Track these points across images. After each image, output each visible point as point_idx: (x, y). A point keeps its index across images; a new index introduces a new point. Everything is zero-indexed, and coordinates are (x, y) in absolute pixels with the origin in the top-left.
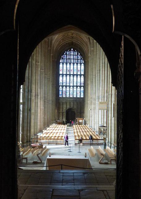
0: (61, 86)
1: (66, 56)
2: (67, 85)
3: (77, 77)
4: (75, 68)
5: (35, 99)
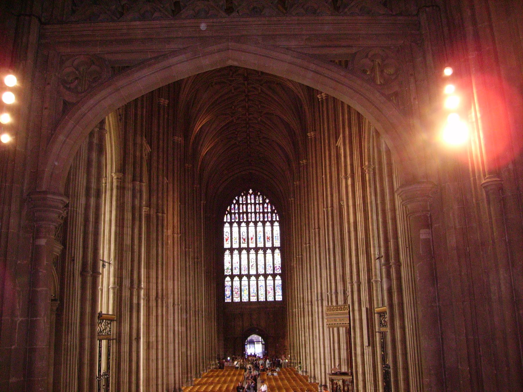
0: (229, 276)
1: (236, 206)
2: (243, 273)
3: (265, 254)
4: (260, 234)
5: (157, 306)
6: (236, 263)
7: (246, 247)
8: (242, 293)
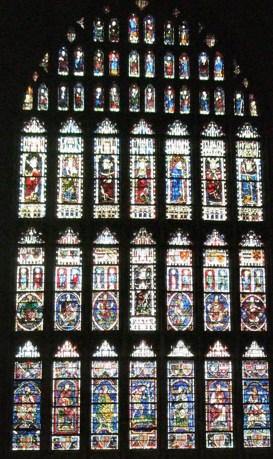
2: (98, 326)
7: (116, 216)
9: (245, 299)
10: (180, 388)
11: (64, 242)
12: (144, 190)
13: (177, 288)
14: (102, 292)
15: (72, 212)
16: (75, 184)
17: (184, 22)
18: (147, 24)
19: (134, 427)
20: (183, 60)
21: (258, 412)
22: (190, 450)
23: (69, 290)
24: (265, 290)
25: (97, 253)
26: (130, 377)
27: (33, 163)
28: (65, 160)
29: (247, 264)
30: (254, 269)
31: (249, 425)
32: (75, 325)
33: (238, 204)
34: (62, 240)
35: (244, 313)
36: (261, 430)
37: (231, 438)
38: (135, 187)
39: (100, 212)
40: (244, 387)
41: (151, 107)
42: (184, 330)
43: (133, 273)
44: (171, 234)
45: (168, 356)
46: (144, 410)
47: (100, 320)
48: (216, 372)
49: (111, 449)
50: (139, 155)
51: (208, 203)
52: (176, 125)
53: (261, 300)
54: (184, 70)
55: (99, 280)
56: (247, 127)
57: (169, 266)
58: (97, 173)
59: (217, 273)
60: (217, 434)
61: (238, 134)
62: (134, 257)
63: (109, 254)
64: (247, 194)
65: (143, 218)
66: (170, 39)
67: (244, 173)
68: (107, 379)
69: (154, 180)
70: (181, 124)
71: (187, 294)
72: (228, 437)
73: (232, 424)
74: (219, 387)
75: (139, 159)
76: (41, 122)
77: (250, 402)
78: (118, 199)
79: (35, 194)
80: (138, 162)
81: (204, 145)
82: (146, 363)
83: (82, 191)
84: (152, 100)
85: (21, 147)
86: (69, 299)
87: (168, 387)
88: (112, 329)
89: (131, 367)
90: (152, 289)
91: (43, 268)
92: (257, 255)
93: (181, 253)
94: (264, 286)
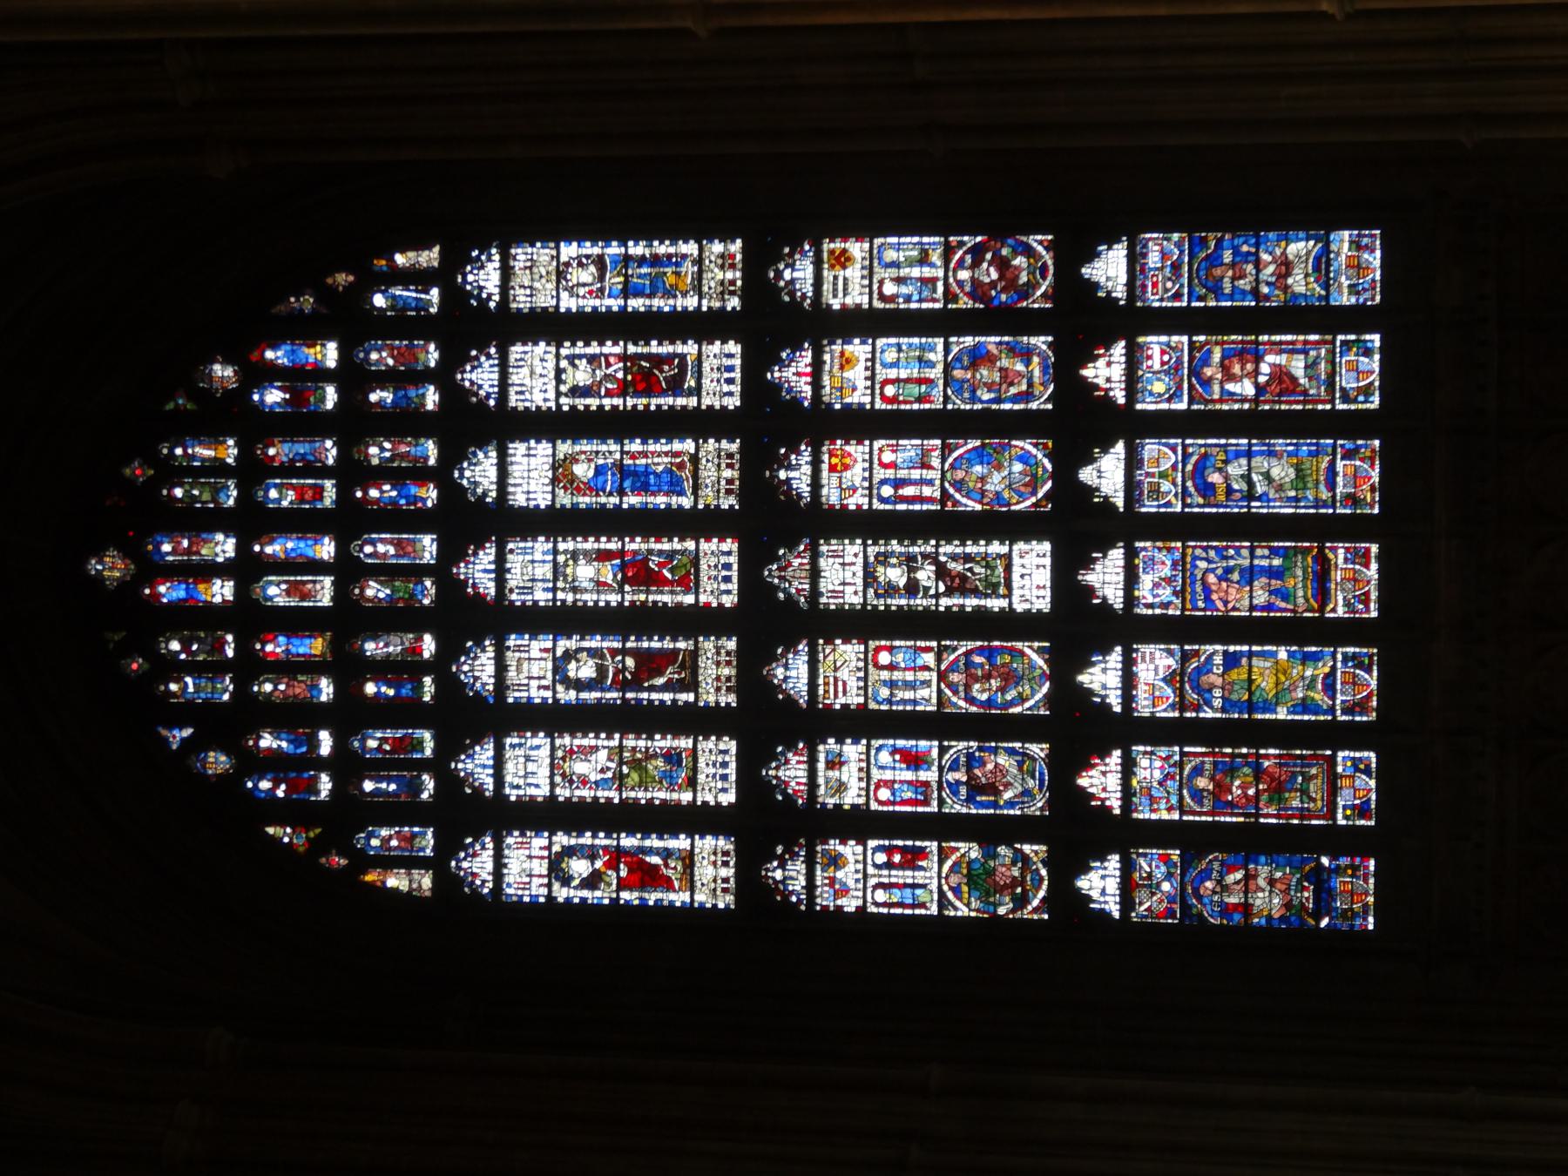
0: (1067, 865)
2: (1034, 699)
6: (930, 775)
7: (732, 644)
8: (1282, 714)
9: (961, 295)
10: (1210, 480)
11: (802, 788)
12: (656, 569)
13: (930, 483)
14: (943, 686)
15: (718, 765)
16: (639, 756)
17: (165, 451)
18: (174, 552)
19: (1316, 606)
20: (278, 453)
21: (1281, 264)
22: (1384, 453)
23: (937, 774)
24: (937, 239)
25: (832, 696)
26: (1178, 613)
27: (579, 867)
28: (571, 782)
29: (863, 286)
30: (877, 268)
31: (1318, 289)
32: (1033, 759)
33: (691, 309)
34: (799, 791)
35: (1004, 297)
36: (1332, 256)
37: (1353, 341)
38: (648, 592)
39: (718, 689)
40: (1212, 304)
41: (418, 546)
42: (1049, 466)
43: (889, 601)
44: (782, 497)
45: (1121, 510)
46: (1270, 578)
47: (1019, 693)
48: (1167, 379)
49: (1375, 668)
50: (555, 580)
51: (690, 393)
52: (468, 479)
53: (965, 248)
54: (305, 454)
55: (909, 695)
56: (470, 278)
57: (870, 503)
58: (609, 695)
59: (889, 371)
60: (1341, 380)
61: (492, 305)
62: (843, 597)
63: (835, 666)
64: (664, 282)
65: (736, 573)
66: (217, 490)
67: (602, 290)
68: (1182, 674)
69: (627, 539)
70: (465, 465)
71: (949, 455)
72: (1349, 349)
73: (1313, 337)
74: (1208, 372)
75: (565, 580)
76: (465, 848)
77: (1254, 284)
78: (681, 638)
79: (666, 865)
80: (577, 584)
81: (523, 401)
82: (1141, 570)
83: (658, 737)
84: (398, 544)
85: (533, 900)
86: (961, 776)
87: (1207, 510)
88: (1046, 661)
89: (1150, 612)
90: (934, 550)
91: (872, 843)
92: (838, 259)
93: (832, 469)
94: (926, 240)
